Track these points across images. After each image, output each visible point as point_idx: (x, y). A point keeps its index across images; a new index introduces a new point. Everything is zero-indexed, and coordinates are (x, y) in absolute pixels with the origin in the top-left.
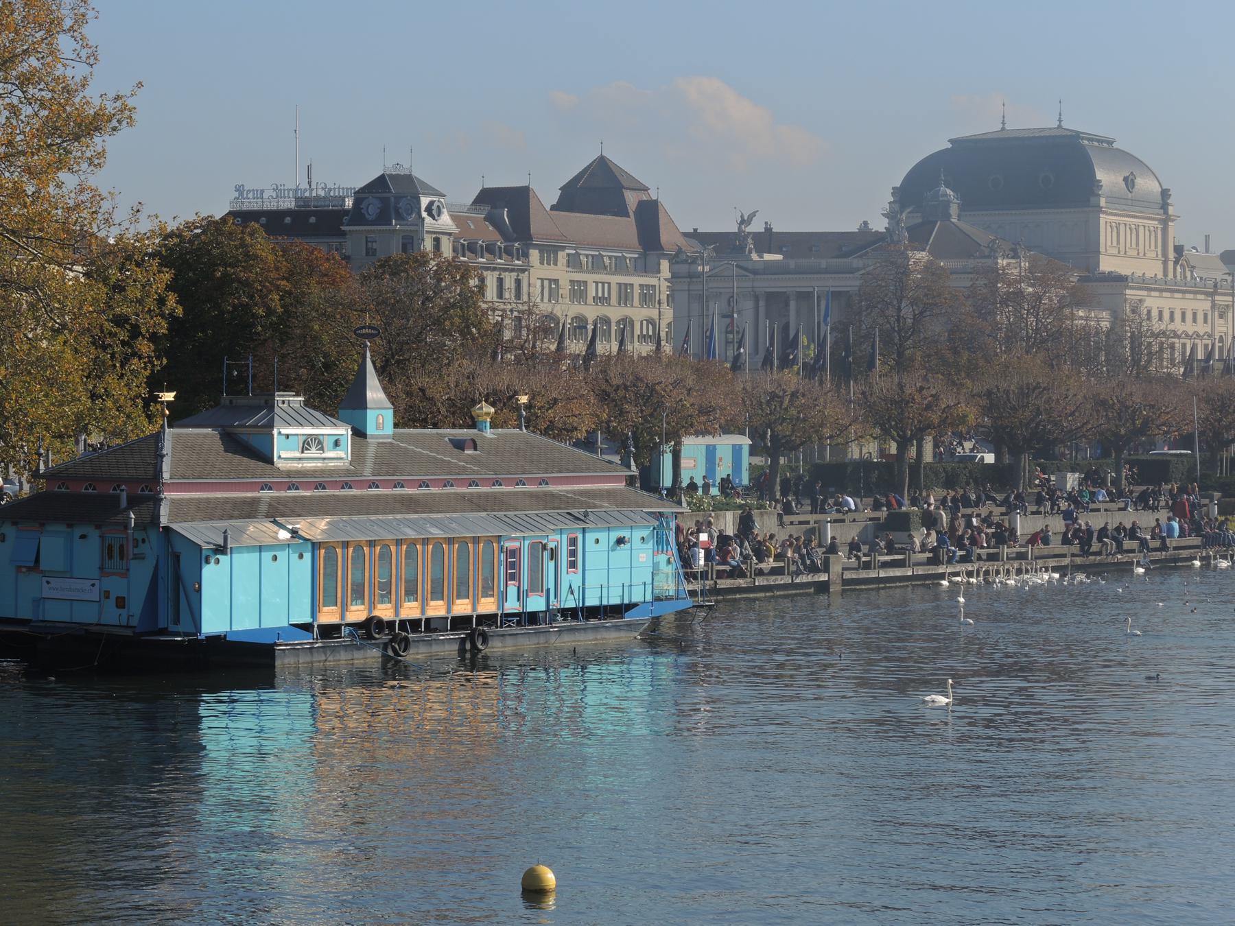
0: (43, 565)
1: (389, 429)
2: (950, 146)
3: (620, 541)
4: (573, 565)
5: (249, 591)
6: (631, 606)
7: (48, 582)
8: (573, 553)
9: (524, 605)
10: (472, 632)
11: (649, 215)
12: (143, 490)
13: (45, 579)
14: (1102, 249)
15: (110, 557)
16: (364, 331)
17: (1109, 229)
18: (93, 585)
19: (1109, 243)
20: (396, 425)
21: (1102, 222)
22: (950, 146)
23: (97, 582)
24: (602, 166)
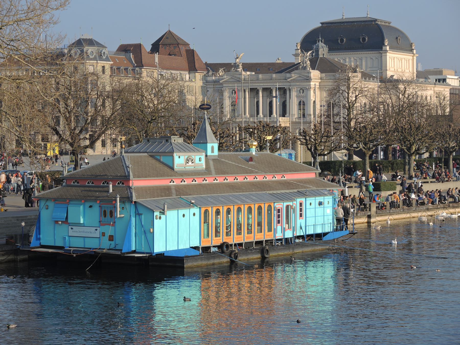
1: (216, 152)
2: (321, 25)
3: (320, 204)
4: (301, 215)
5: (176, 231)
6: (325, 234)
7: (72, 229)
8: (301, 210)
9: (284, 235)
11: (191, 54)
12: (103, 183)
13: (70, 227)
14: (388, 69)
15: (105, 216)
16: (204, 107)
17: (398, 61)
18: (96, 230)
19: (390, 66)
20: (219, 150)
22: (321, 25)
23: (98, 228)
24: (169, 34)
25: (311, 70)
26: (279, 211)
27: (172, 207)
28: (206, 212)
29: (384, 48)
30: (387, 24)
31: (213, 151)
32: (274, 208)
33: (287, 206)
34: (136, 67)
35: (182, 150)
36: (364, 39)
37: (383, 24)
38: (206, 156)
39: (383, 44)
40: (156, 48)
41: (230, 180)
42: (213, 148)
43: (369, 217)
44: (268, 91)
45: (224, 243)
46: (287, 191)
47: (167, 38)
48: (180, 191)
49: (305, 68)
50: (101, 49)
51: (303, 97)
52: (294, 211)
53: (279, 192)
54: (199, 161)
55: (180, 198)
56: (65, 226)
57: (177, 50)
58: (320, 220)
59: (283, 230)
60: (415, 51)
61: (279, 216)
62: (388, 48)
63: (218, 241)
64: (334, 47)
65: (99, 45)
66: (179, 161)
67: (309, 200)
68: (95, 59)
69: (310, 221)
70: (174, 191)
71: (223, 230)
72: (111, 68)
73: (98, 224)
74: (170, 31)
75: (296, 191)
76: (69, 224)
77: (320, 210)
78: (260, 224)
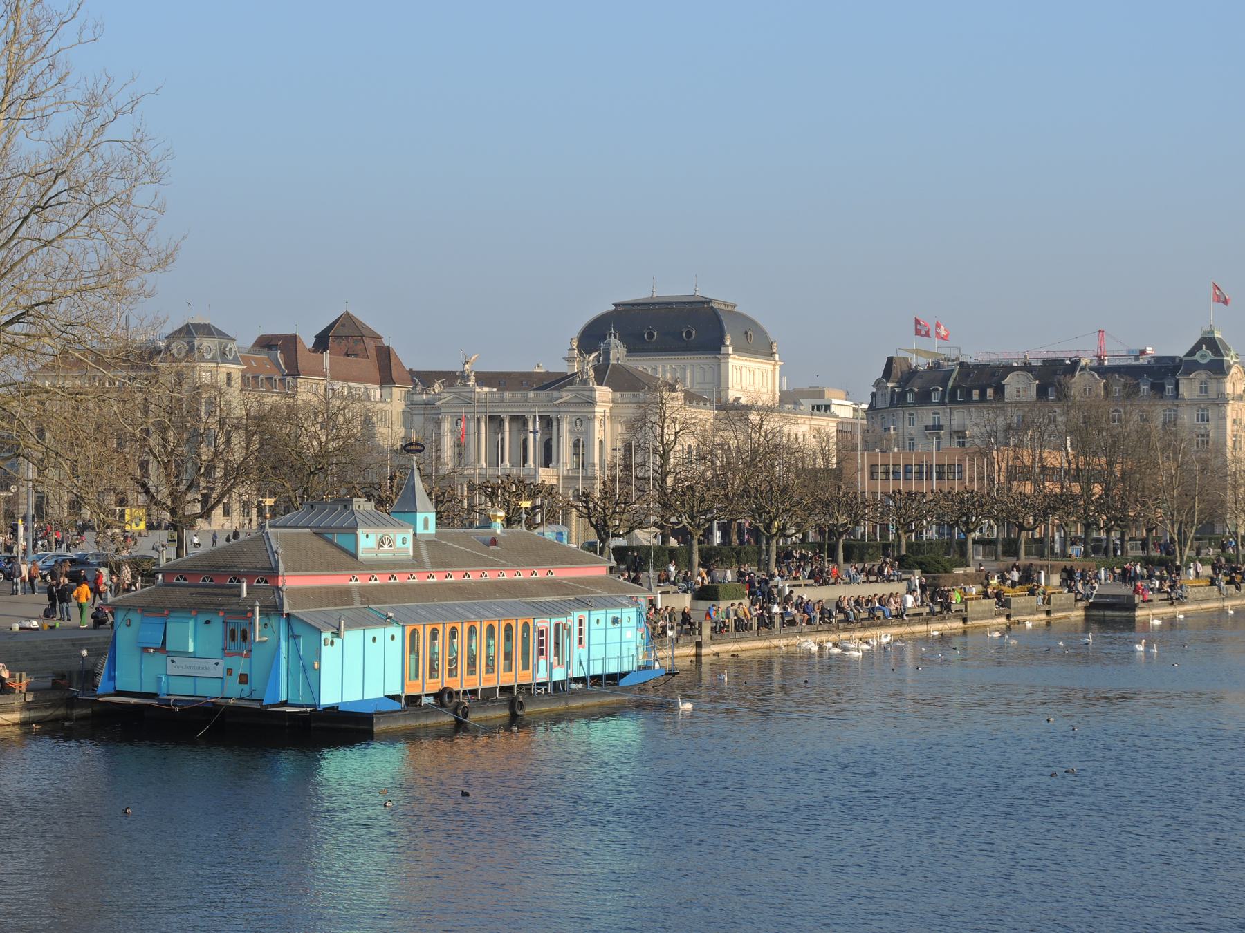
0: (168, 648)
1: (432, 529)
3: (615, 621)
4: (580, 641)
5: (359, 668)
6: (623, 675)
9: (551, 676)
10: (513, 698)
11: (385, 355)
13: (169, 659)
20: (439, 523)
25: (596, 387)
26: (542, 633)
27: (355, 623)
28: (414, 633)
29: (723, 349)
31: (426, 527)
32: (534, 627)
33: (557, 625)
35: (373, 523)
36: (689, 334)
38: (415, 534)
39: (723, 343)
40: (322, 342)
41: (456, 577)
42: (426, 520)
43: (699, 645)
44: (520, 421)
45: (445, 689)
46: (557, 598)
47: (343, 325)
48: (369, 595)
51: (581, 433)
52: (569, 634)
53: (542, 599)
54: (401, 543)
55: (366, 608)
56: (161, 657)
57: (360, 346)
58: (614, 651)
59: (550, 667)
60: (777, 356)
61: (542, 643)
62: (731, 349)
63: (434, 686)
64: (637, 345)
65: (221, 335)
66: (367, 542)
67: (597, 614)
68: (213, 360)
69: (597, 652)
70: (357, 597)
71: (443, 666)
72: (243, 377)
73: (220, 655)
74: (347, 313)
75: (571, 598)
76: (168, 653)
77: (614, 633)
78: (508, 656)
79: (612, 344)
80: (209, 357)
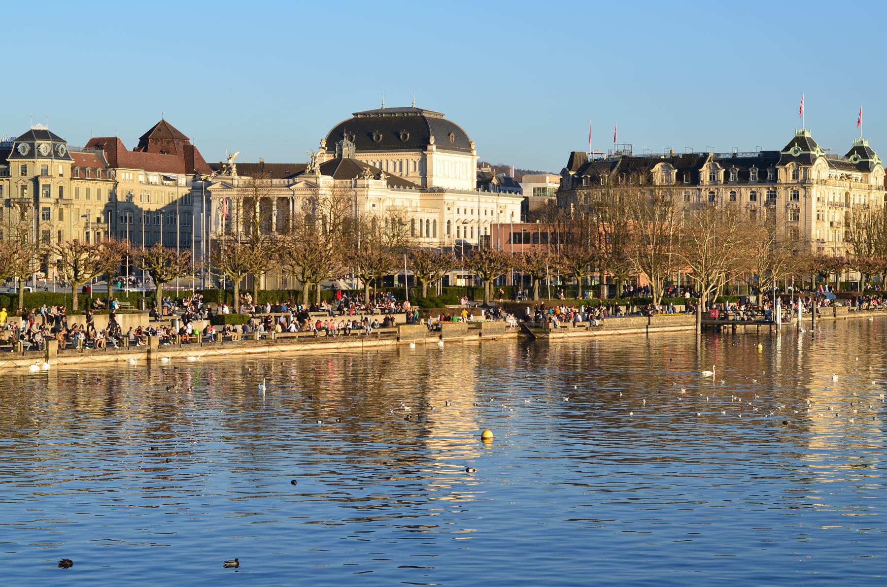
2: (353, 117)
21: (434, 159)
25: (320, 176)
29: (429, 147)
30: (438, 117)
34: (109, 167)
36: (405, 136)
37: (432, 116)
39: (429, 143)
40: (144, 142)
43: (149, 352)
47: (160, 130)
49: (313, 172)
50: (58, 143)
57: (171, 146)
60: (475, 152)
62: (434, 147)
65: (55, 138)
68: (49, 156)
72: (72, 168)
74: (163, 123)
79: (344, 144)
80: (45, 154)
